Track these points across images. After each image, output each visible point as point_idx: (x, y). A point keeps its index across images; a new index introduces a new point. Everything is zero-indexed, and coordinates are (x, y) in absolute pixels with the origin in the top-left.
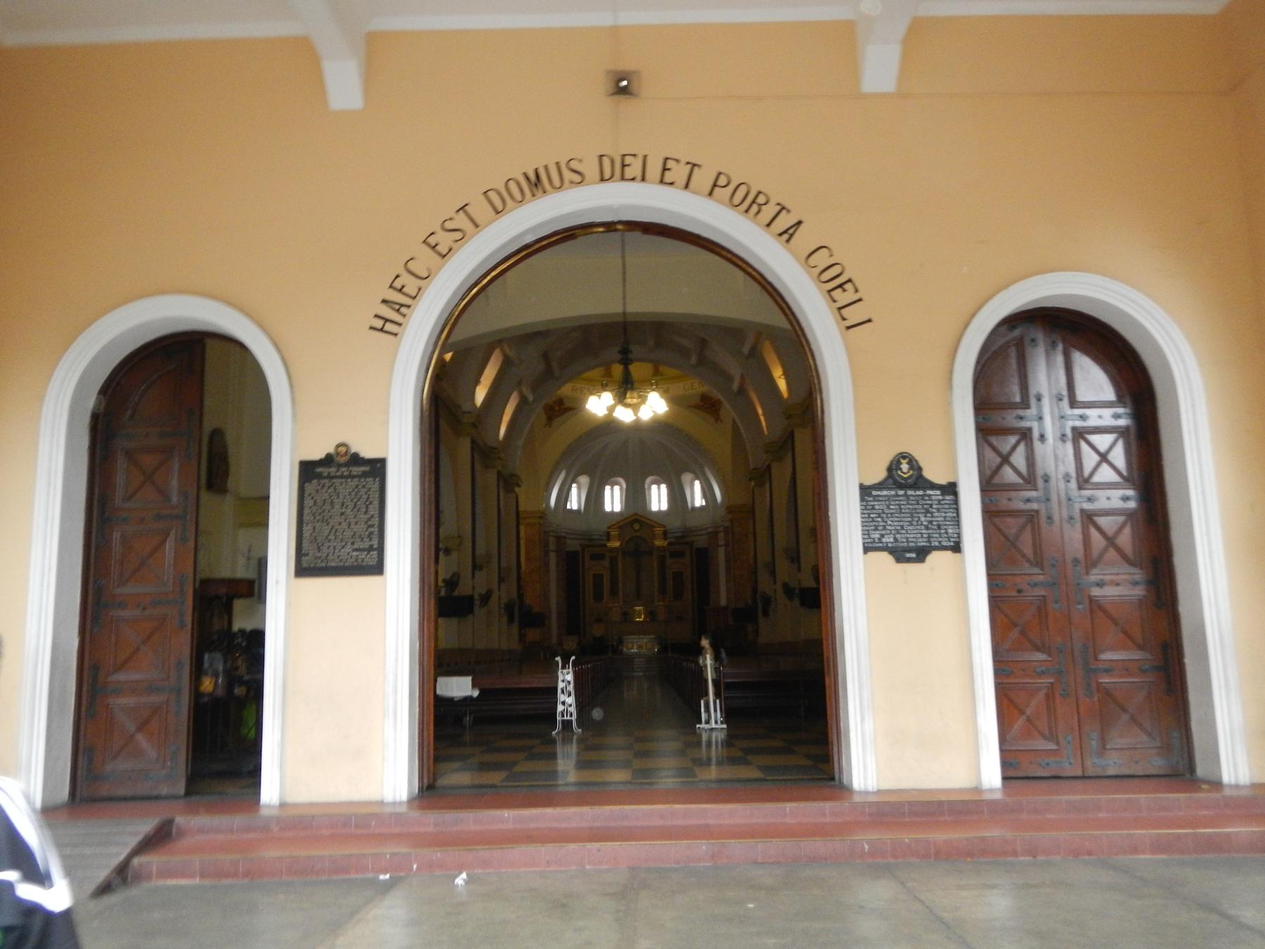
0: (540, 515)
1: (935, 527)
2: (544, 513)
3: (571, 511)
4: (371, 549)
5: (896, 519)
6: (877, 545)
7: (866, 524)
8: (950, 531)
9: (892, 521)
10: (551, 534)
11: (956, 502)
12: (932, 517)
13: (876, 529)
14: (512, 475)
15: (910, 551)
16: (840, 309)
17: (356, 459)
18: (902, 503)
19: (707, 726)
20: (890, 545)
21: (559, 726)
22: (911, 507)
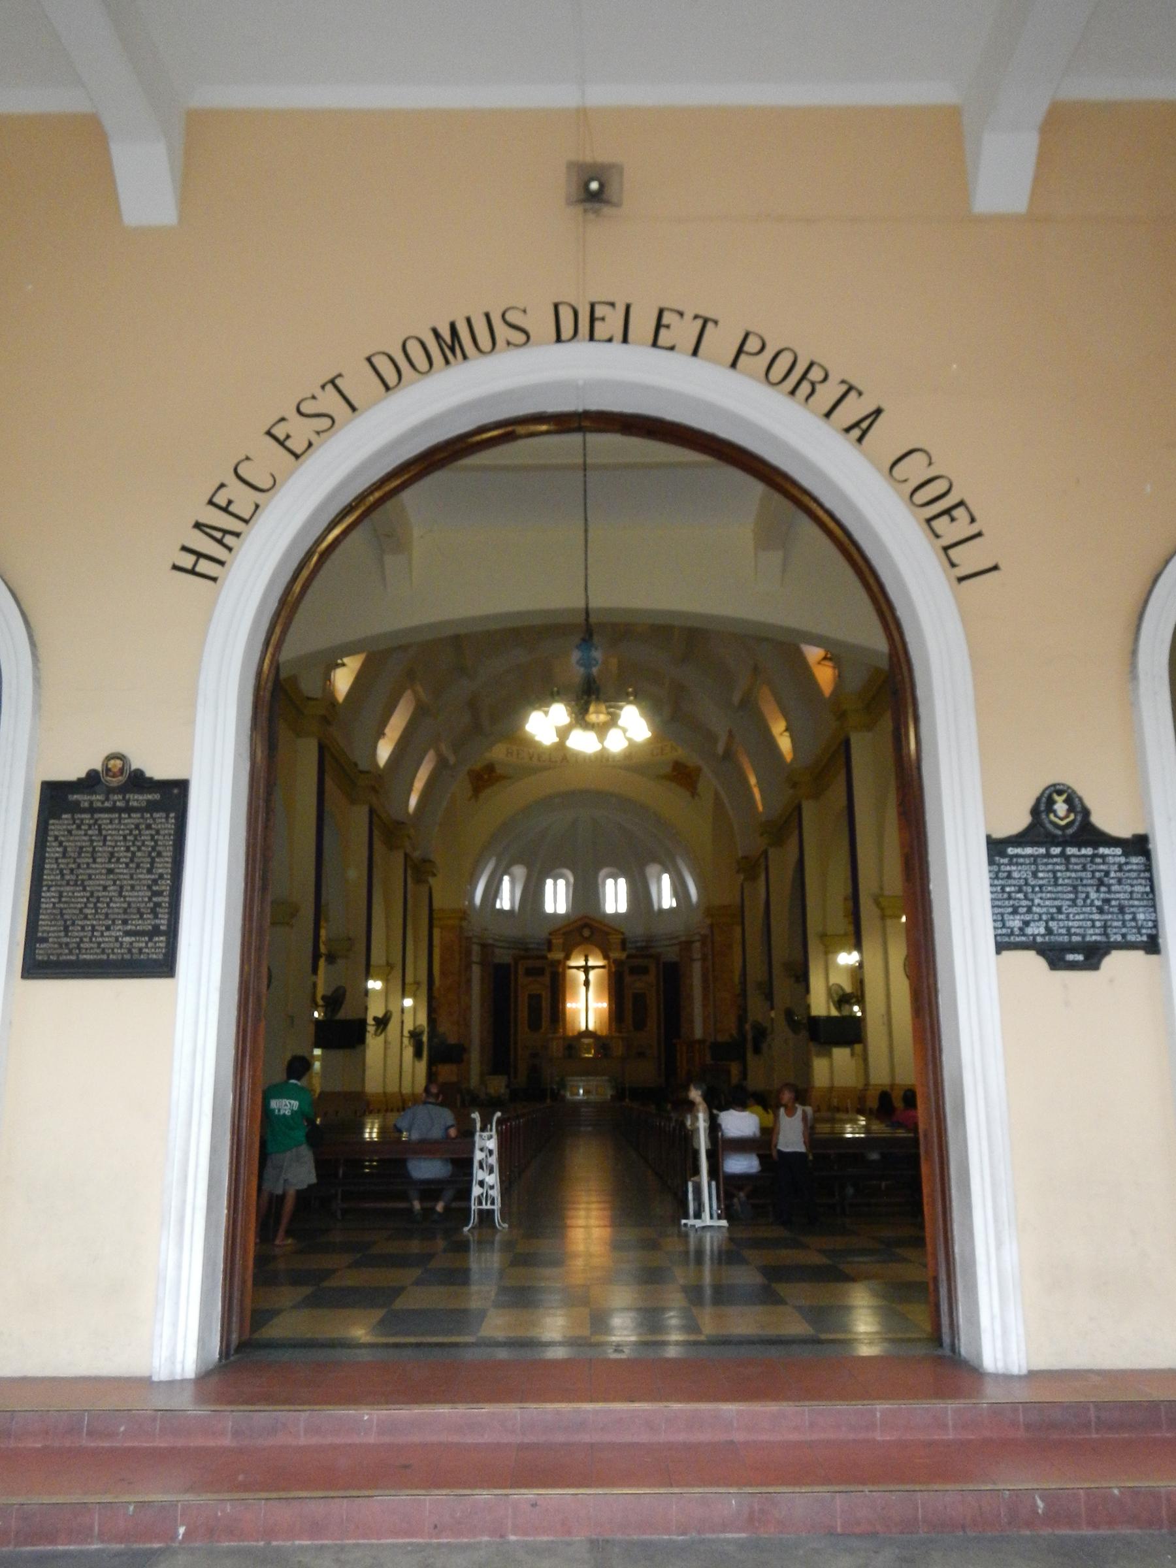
1: (1116, 910)
2: (465, 912)
3: (501, 911)
4: (156, 931)
5: (1049, 895)
6: (1018, 939)
7: (999, 903)
8: (1141, 917)
9: (1041, 898)
10: (475, 940)
11: (1148, 867)
12: (1109, 892)
13: (1015, 912)
14: (425, 861)
15: (1074, 949)
16: (946, 549)
17: (138, 781)
18: (1058, 867)
19: (698, 1223)
20: (1039, 939)
21: (474, 1219)
22: (1073, 875)
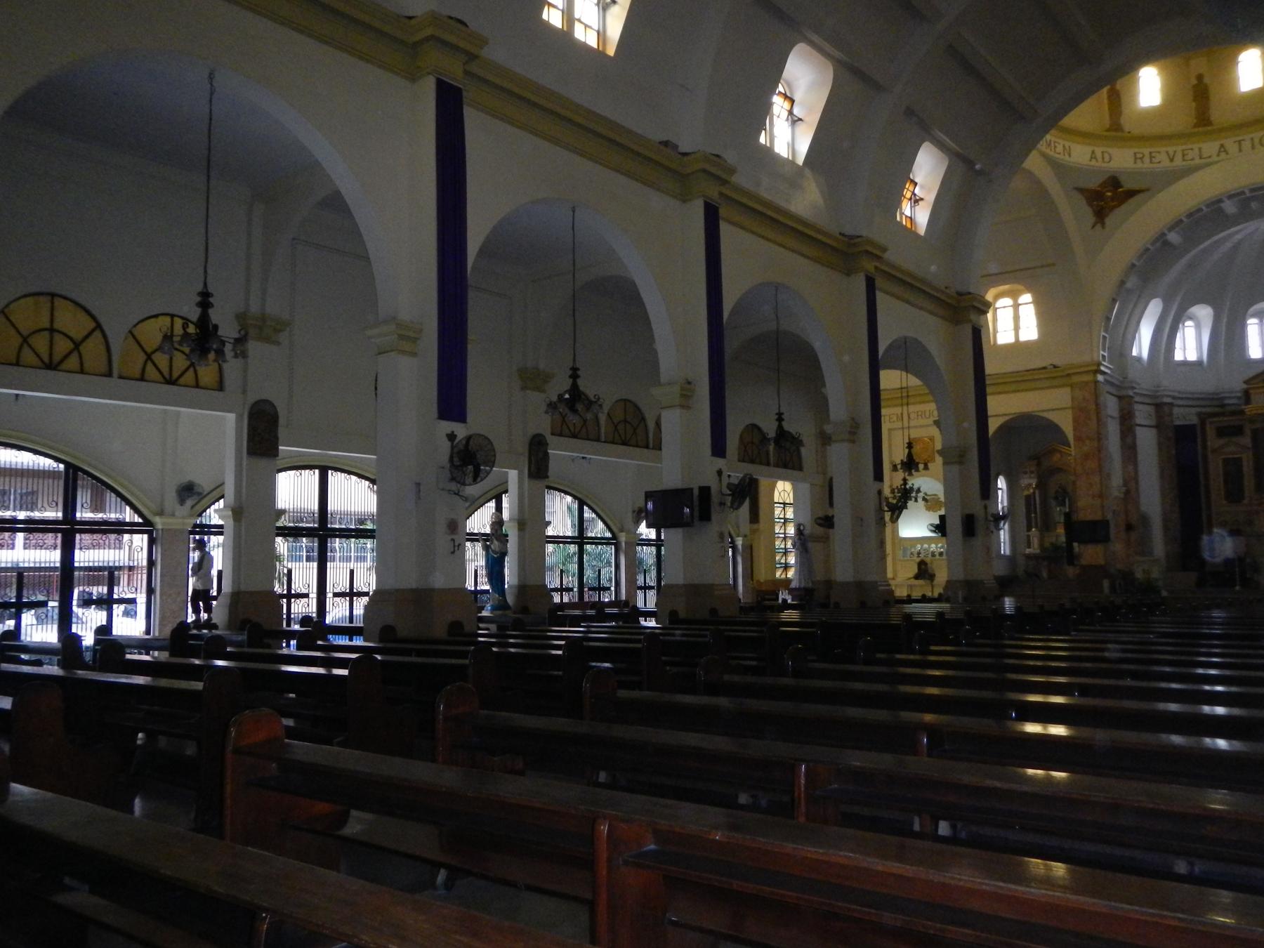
0: (1095, 368)
3: (1185, 363)
